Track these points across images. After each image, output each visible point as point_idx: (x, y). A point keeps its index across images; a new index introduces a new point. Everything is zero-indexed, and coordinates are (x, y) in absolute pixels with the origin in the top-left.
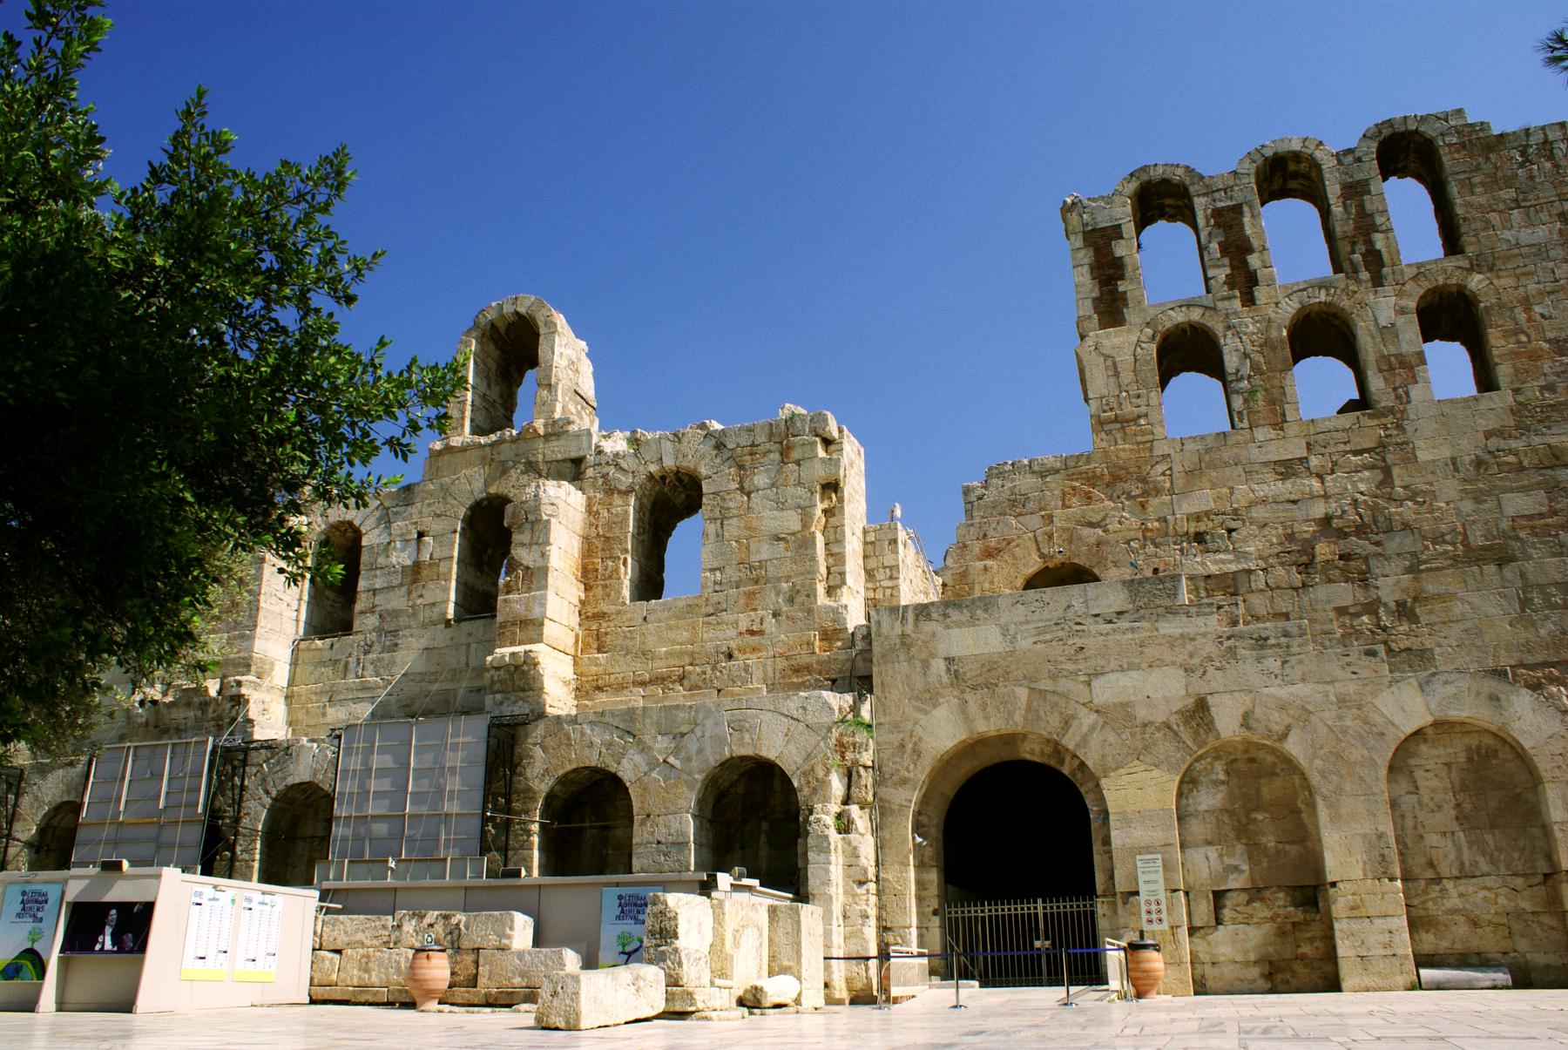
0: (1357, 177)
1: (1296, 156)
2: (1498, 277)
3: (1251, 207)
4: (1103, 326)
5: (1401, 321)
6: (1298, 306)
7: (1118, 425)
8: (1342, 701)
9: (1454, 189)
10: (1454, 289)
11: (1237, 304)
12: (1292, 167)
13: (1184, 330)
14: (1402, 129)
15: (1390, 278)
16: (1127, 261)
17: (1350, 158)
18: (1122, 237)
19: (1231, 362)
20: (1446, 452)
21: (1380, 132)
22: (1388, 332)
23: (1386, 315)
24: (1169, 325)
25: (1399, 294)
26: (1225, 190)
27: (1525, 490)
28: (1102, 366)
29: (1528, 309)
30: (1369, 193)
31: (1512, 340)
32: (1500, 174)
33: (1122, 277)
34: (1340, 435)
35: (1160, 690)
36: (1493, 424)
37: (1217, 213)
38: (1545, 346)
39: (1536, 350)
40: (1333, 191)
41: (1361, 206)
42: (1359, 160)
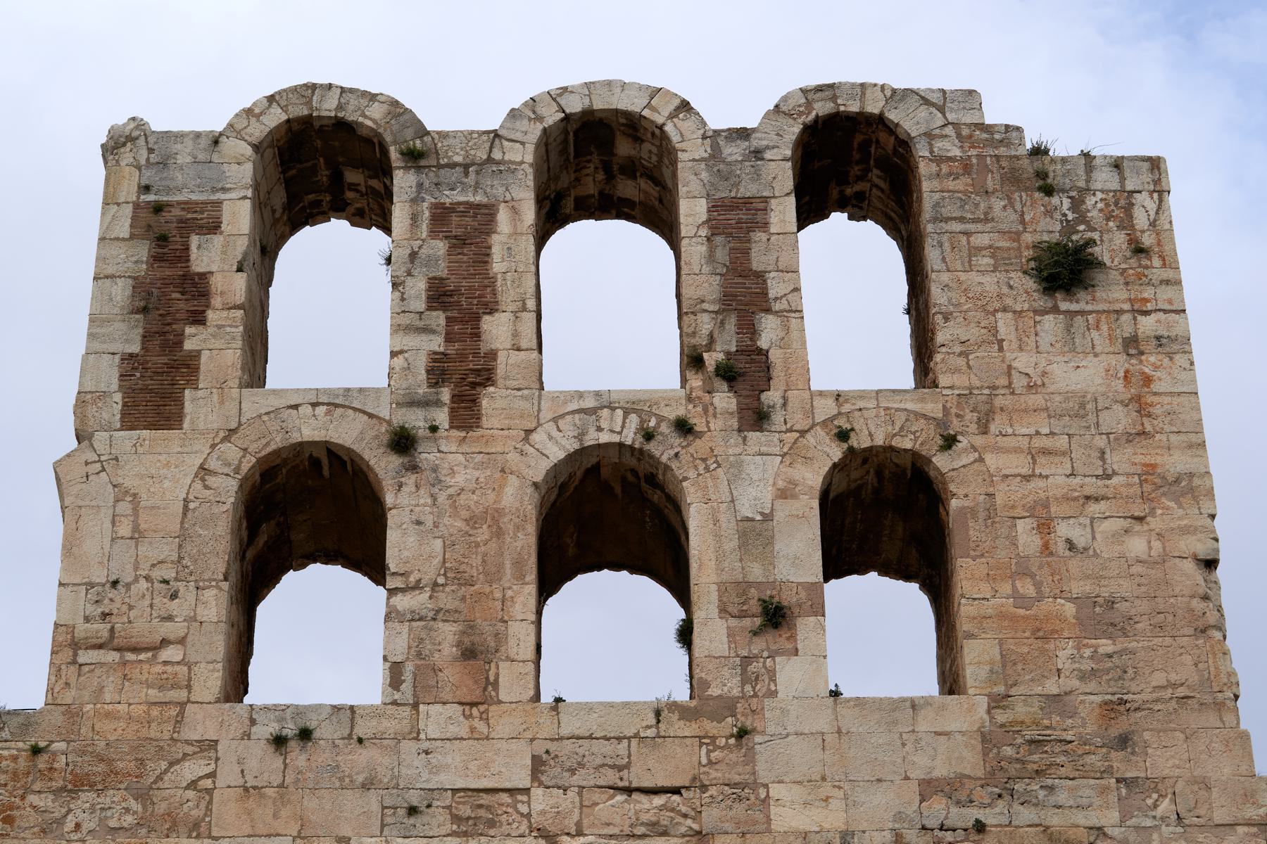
0: (748, 189)
1: (633, 125)
2: (997, 449)
3: (515, 211)
4: (131, 419)
5: (784, 511)
6: (573, 446)
7: (112, 656)
10: (907, 462)
11: (442, 417)
12: (624, 148)
13: (315, 463)
14: (854, 107)
15: (777, 418)
16: (217, 282)
17: (733, 151)
18: (214, 227)
19: (400, 545)
20: (833, 819)
21: (809, 104)
22: (755, 534)
23: (754, 495)
24: (278, 442)
25: (790, 455)
26: (466, 167)
28: (106, 515)
29: (1045, 527)
30: (765, 226)
31: (1006, 588)
33: (198, 318)
34: (607, 748)
36: (941, 771)
38: (1070, 609)
39: (1048, 618)
40: (692, 211)
41: (740, 255)
42: (758, 154)
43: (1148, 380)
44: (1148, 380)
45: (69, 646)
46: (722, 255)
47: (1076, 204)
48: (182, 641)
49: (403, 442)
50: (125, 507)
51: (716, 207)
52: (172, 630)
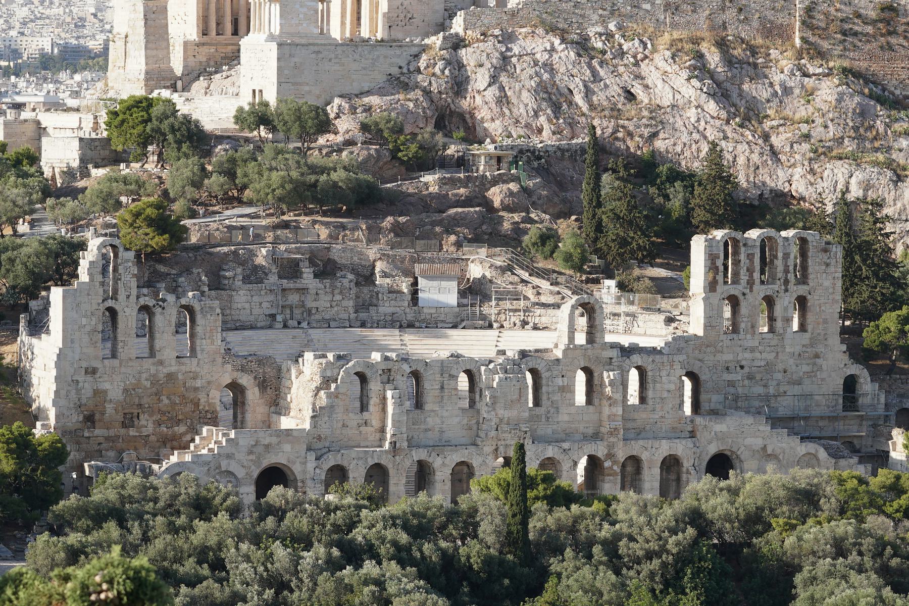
4: (710, 292)
8: (791, 448)
9: (810, 262)
20: (792, 350)
25: (791, 296)
27: (808, 364)
35: (758, 443)
37: (748, 255)
45: (705, 326)
49: (744, 294)
51: (784, 254)
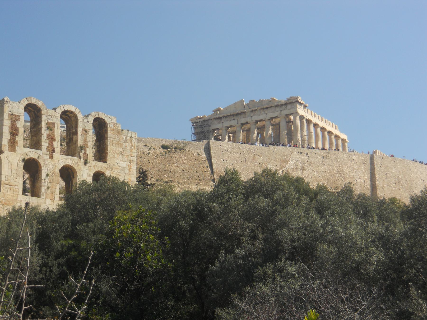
4: (10, 150)
25: (90, 170)
32: (120, 142)
37: (48, 123)
43: (131, 167)
44: (131, 167)
46: (83, 138)
47: (126, 138)
48: (17, 186)
50: (10, 164)
52: (17, 183)
